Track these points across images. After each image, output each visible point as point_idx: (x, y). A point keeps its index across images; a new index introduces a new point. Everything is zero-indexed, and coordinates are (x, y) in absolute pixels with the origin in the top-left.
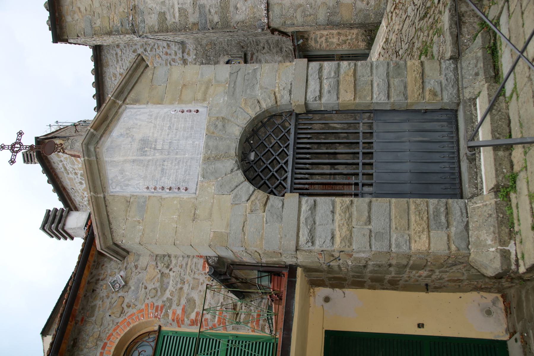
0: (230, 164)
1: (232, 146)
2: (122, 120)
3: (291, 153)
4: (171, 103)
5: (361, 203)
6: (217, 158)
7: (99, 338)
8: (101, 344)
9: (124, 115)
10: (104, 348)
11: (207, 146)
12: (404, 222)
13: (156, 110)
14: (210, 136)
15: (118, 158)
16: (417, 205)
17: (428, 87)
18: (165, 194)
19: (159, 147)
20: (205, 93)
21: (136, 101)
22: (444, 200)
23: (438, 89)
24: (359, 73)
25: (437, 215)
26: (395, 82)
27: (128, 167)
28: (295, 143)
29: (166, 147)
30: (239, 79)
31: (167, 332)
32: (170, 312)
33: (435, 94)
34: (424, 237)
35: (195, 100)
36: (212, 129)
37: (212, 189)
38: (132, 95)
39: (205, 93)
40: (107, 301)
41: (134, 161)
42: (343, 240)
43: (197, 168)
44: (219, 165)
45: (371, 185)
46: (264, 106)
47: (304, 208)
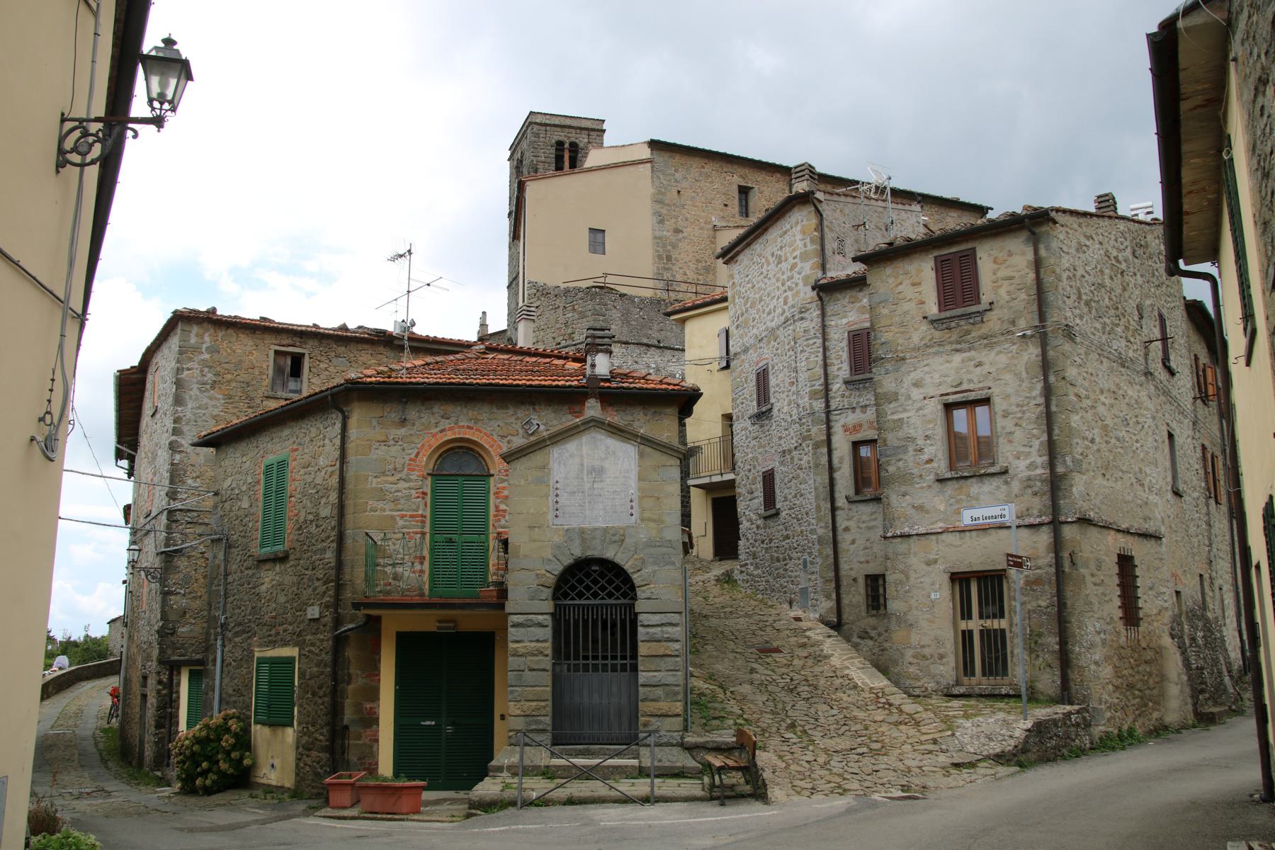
0: (578, 552)
1: (595, 553)
2: (623, 444)
3: (597, 602)
4: (639, 489)
5: (547, 663)
6: (583, 540)
7: (477, 421)
8: (471, 424)
9: (628, 446)
10: (469, 427)
11: (596, 529)
12: (530, 697)
13: (633, 476)
14: (606, 530)
15: (585, 450)
16: (544, 707)
17: (653, 720)
18: (551, 499)
19: (596, 485)
20: (650, 520)
21: (641, 455)
22: (549, 728)
23: (650, 728)
24: (668, 659)
25: (536, 722)
26: (659, 692)
27: (577, 460)
28: (607, 605)
29: (596, 492)
30: (665, 550)
31: (489, 483)
32: (505, 484)
33: (645, 725)
34: (518, 712)
35: (643, 510)
36: (612, 532)
37: (557, 539)
38: (648, 450)
39: (650, 520)
40: (512, 420)
41: (582, 465)
42: (515, 649)
43: (575, 523)
44: (577, 542)
45: (569, 670)
46: (634, 577)
47: (540, 617)
